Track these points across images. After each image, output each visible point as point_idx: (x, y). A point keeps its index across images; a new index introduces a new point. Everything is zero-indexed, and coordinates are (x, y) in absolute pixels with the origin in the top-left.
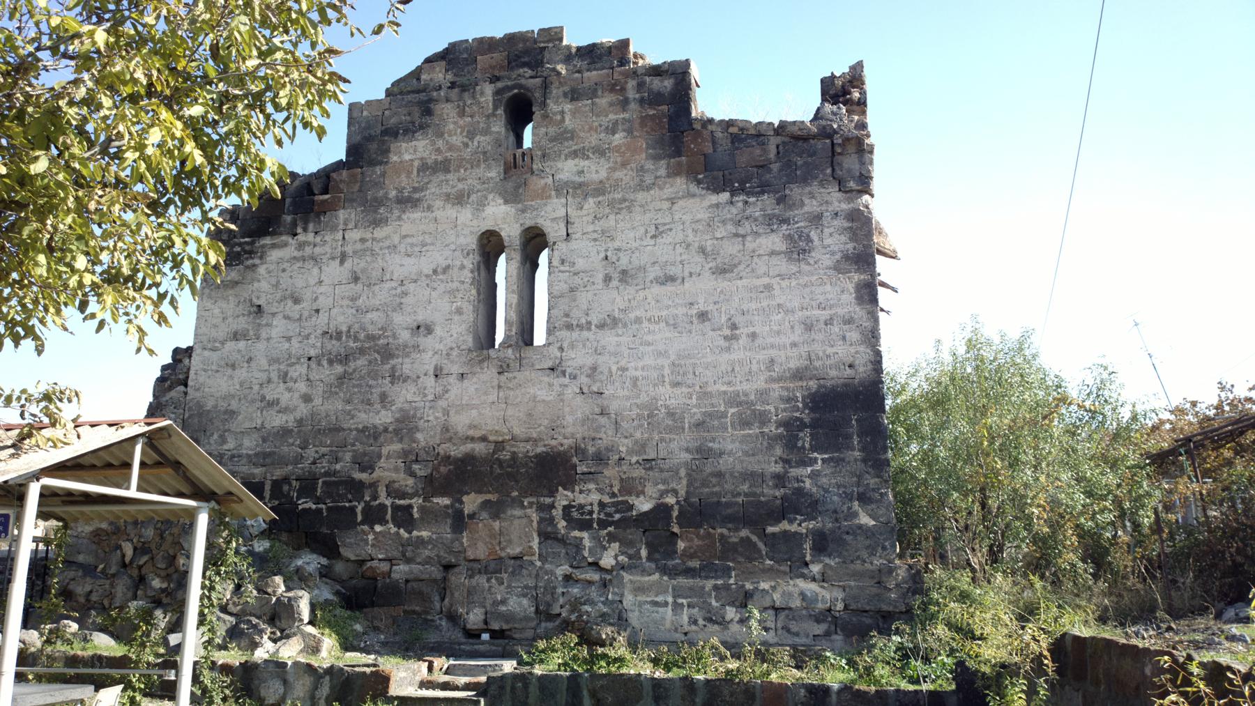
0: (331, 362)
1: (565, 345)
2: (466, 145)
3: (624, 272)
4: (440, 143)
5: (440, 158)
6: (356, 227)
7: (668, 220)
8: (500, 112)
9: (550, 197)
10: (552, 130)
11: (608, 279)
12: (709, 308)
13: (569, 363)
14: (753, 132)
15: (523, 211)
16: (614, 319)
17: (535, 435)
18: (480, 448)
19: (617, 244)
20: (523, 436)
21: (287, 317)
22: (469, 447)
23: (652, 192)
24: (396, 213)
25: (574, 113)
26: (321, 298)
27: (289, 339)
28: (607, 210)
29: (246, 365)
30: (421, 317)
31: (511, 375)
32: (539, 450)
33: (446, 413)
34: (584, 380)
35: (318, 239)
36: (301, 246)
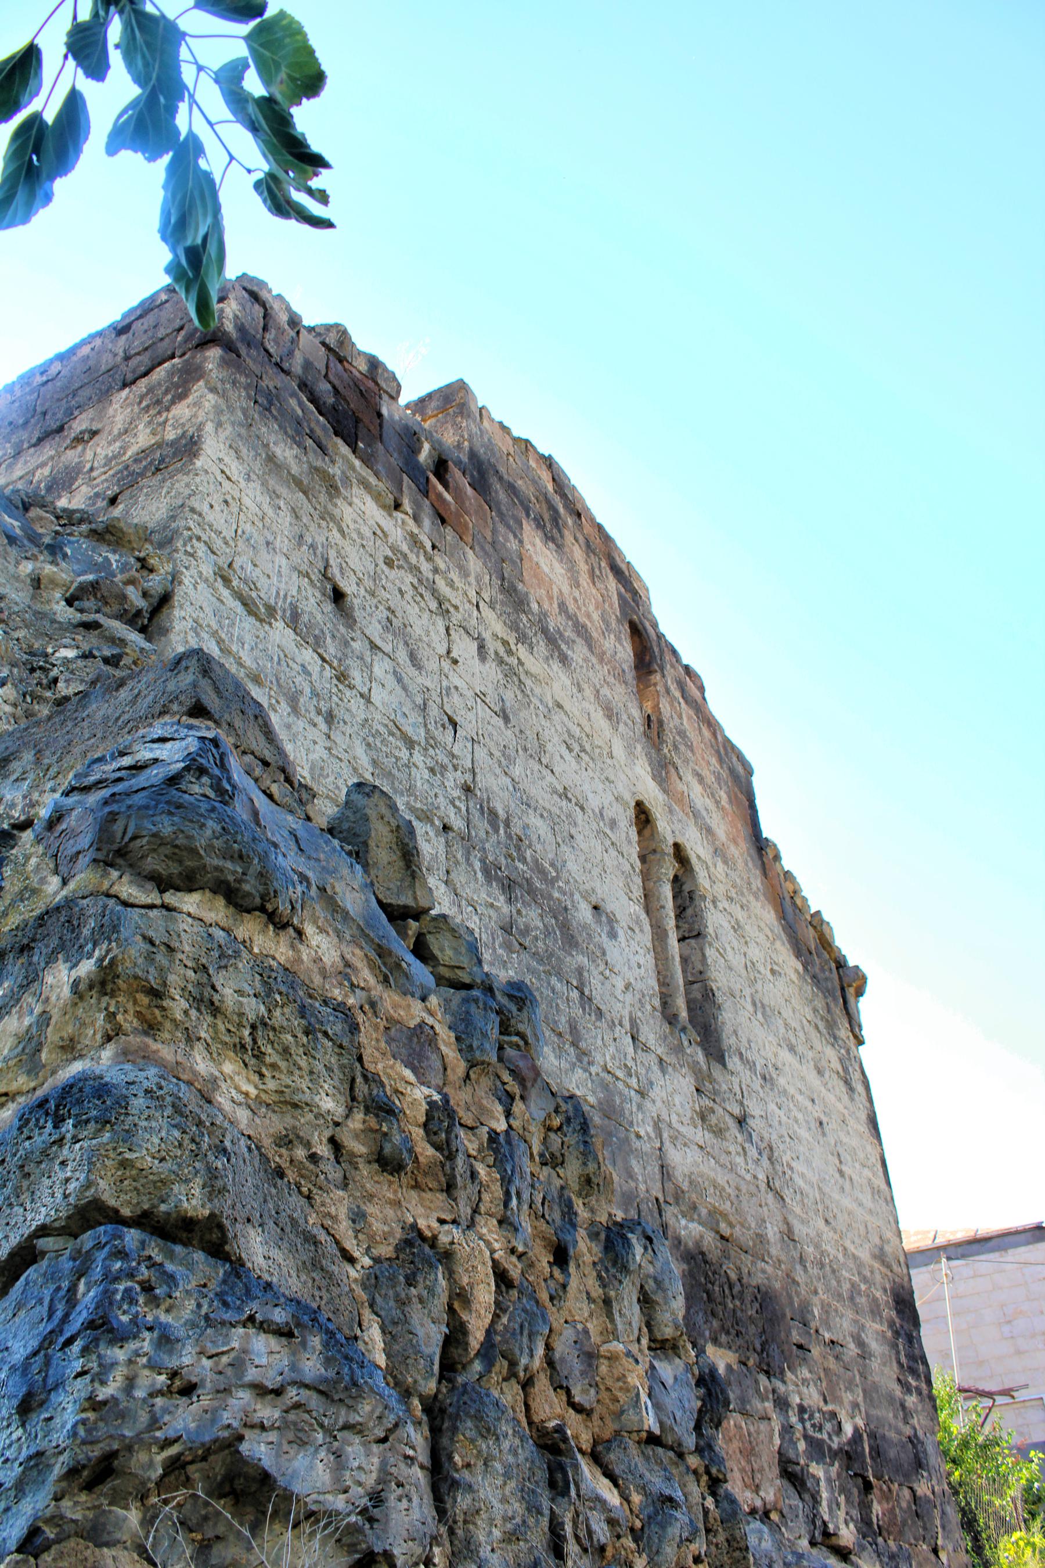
0: (486, 871)
1: (744, 1087)
3: (763, 1006)
6: (492, 606)
8: (627, 627)
11: (754, 1004)
12: (825, 1120)
14: (799, 902)
18: (709, 1240)
21: (399, 680)
23: (759, 904)
24: (542, 647)
25: (689, 718)
26: (455, 698)
27: (410, 744)
29: (323, 726)
32: (758, 1279)
34: (765, 1162)
35: (441, 562)
36: (415, 541)
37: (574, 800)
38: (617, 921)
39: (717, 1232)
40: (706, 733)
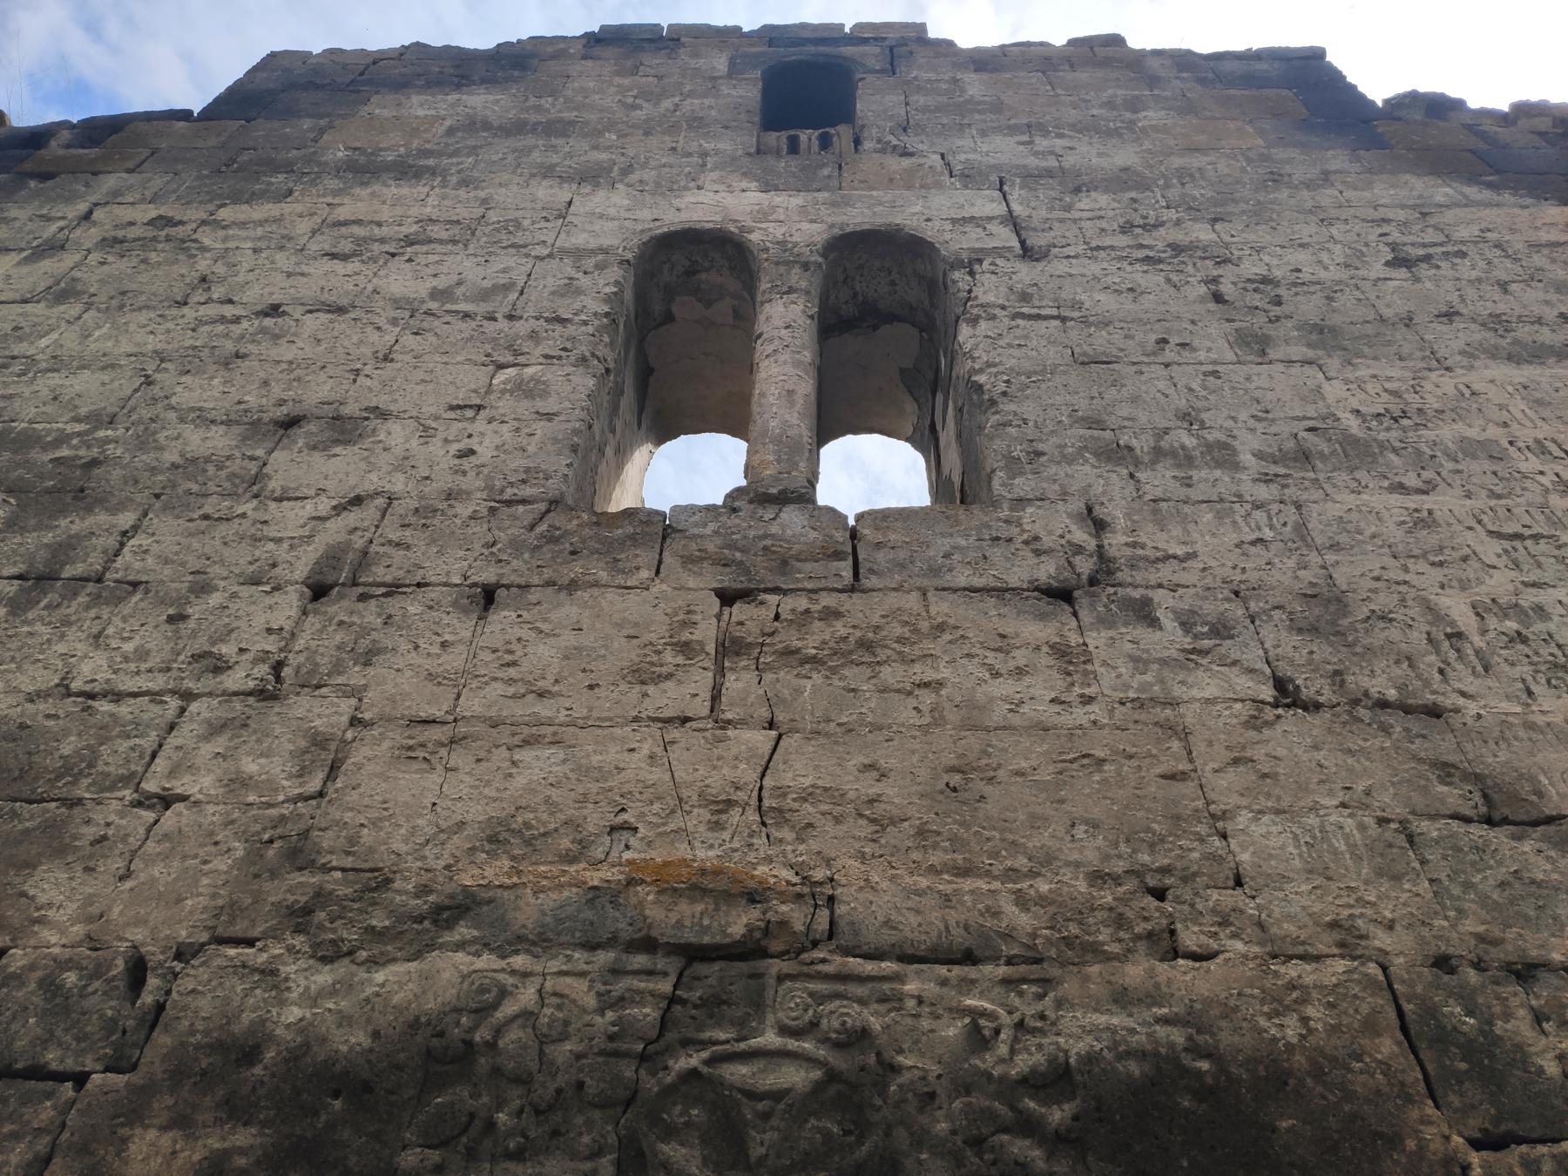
1: (1115, 512)
2: (634, 107)
4: (546, 102)
5: (534, 117)
7: (1431, 236)
9: (938, 185)
10: (919, 100)
13: (1166, 572)
15: (834, 204)
16: (1349, 441)
17: (1024, 921)
19: (1250, 268)
20: (922, 924)
22: (451, 970)
24: (333, 184)
28: (1172, 214)
30: (318, 391)
31: (802, 603)
33: (327, 756)
37: (297, 312)
38: (384, 415)
39: (648, 945)
40: (1083, 76)
